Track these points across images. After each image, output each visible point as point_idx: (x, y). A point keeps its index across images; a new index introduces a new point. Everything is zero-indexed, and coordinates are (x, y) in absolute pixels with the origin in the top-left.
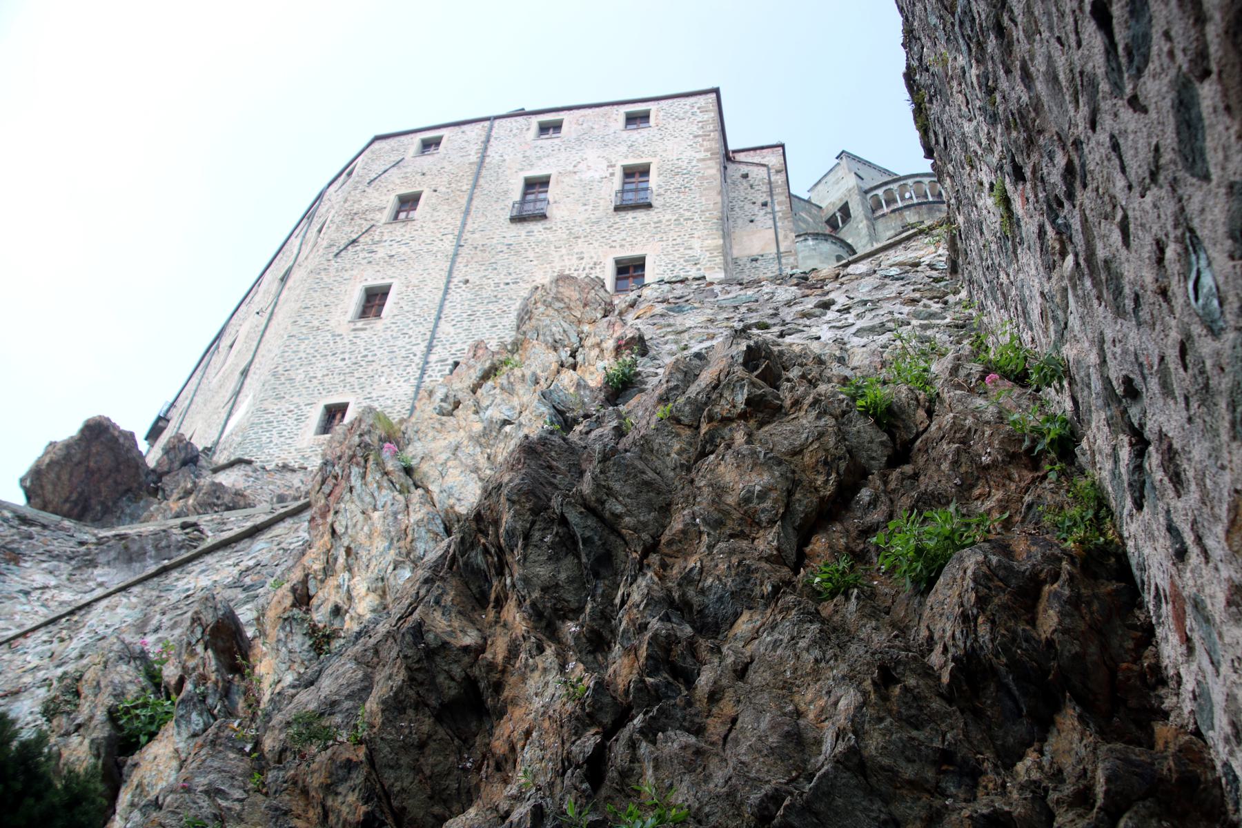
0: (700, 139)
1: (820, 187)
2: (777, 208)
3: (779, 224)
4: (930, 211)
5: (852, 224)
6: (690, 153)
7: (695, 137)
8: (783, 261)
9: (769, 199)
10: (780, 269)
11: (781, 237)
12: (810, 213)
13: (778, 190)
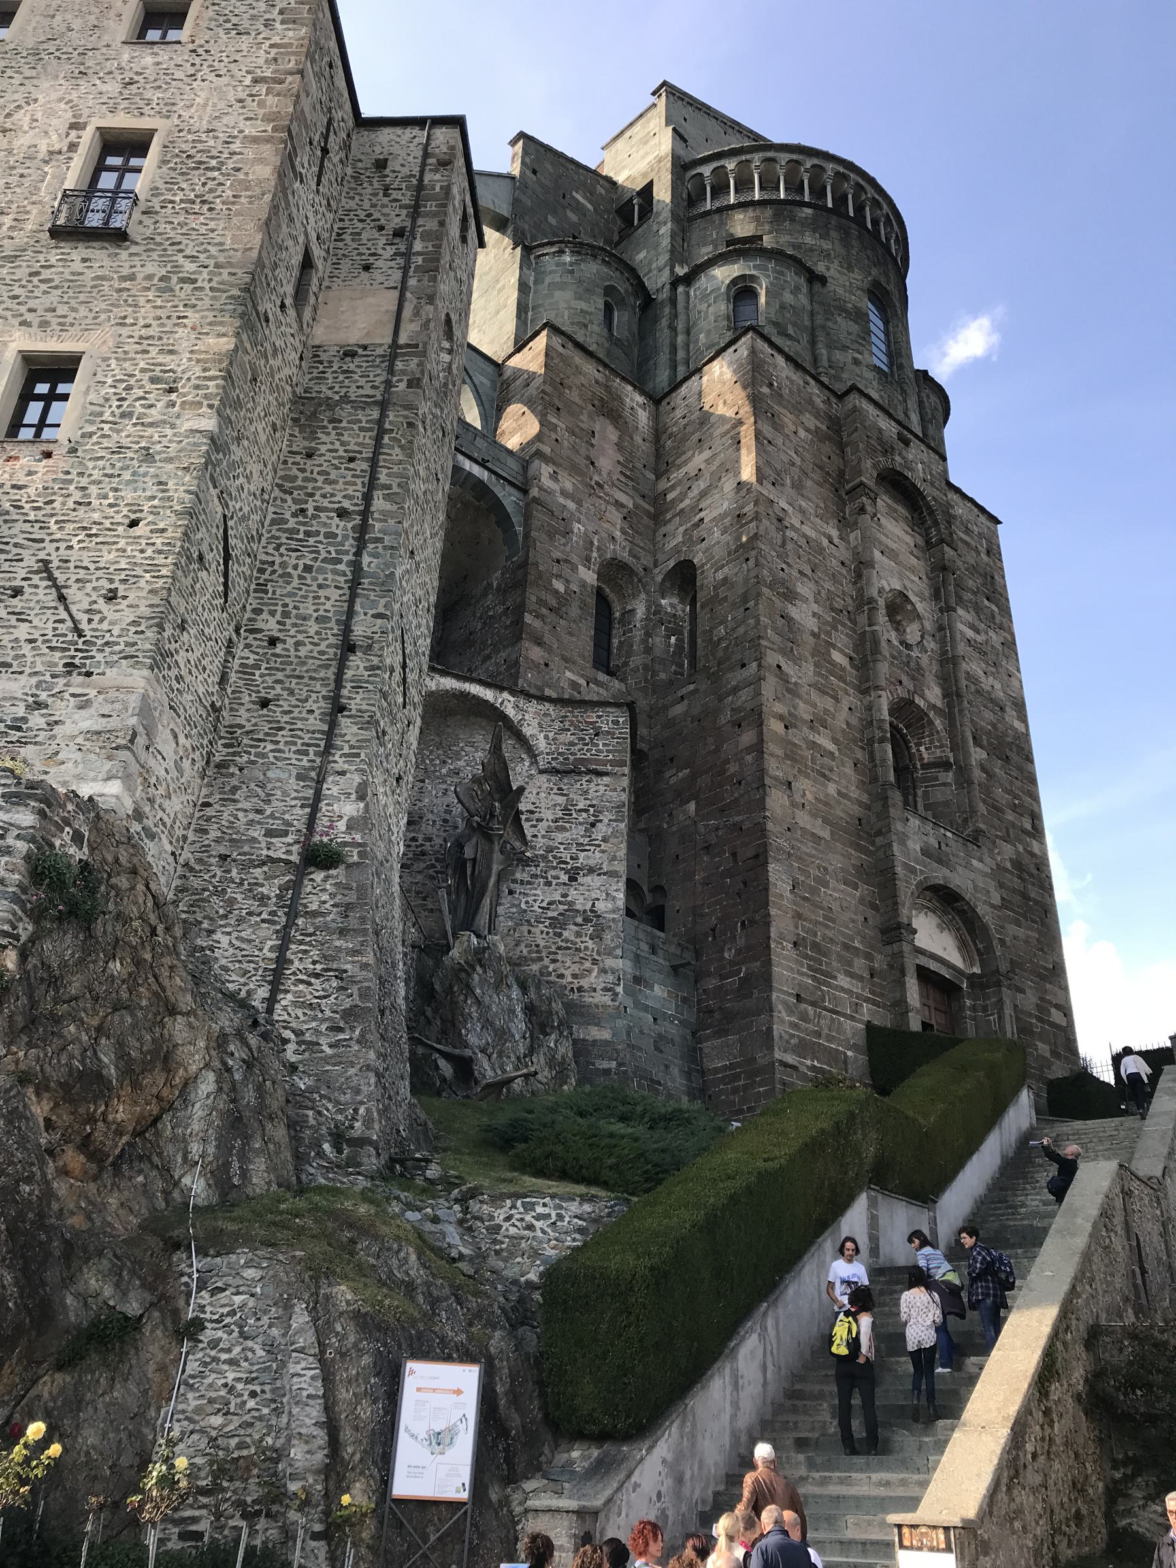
0: (263, 88)
1: (620, 144)
2: (418, 246)
3: (412, 282)
4: (777, 218)
5: (652, 224)
6: (234, 120)
7: (256, 81)
8: (399, 365)
9: (408, 224)
10: (388, 384)
11: (407, 312)
12: (590, 193)
13: (431, 206)
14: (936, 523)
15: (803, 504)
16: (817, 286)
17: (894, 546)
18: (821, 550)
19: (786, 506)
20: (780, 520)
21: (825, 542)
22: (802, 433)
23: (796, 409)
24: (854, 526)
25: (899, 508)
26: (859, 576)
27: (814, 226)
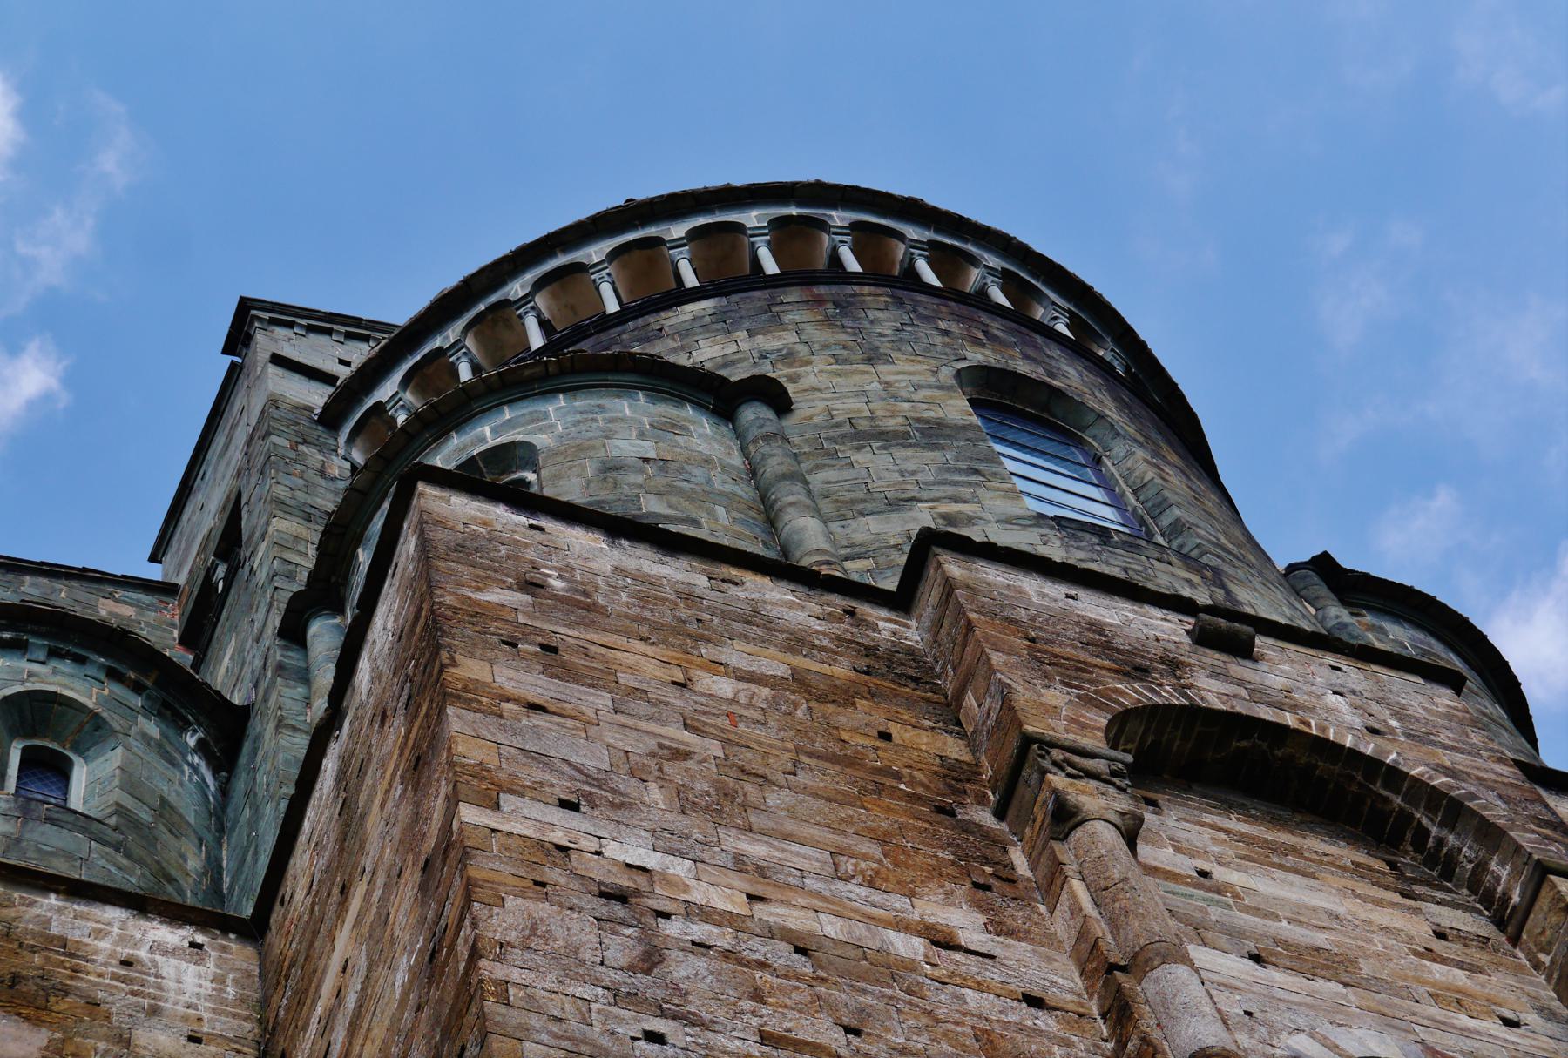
14: (1491, 835)
15: (757, 850)
16: (754, 414)
17: (1321, 939)
18: (892, 970)
19: (652, 860)
20: (621, 897)
21: (910, 947)
22: (725, 687)
23: (686, 633)
24: (1052, 881)
25: (1315, 844)
26: (1120, 1012)
27: (724, 323)
